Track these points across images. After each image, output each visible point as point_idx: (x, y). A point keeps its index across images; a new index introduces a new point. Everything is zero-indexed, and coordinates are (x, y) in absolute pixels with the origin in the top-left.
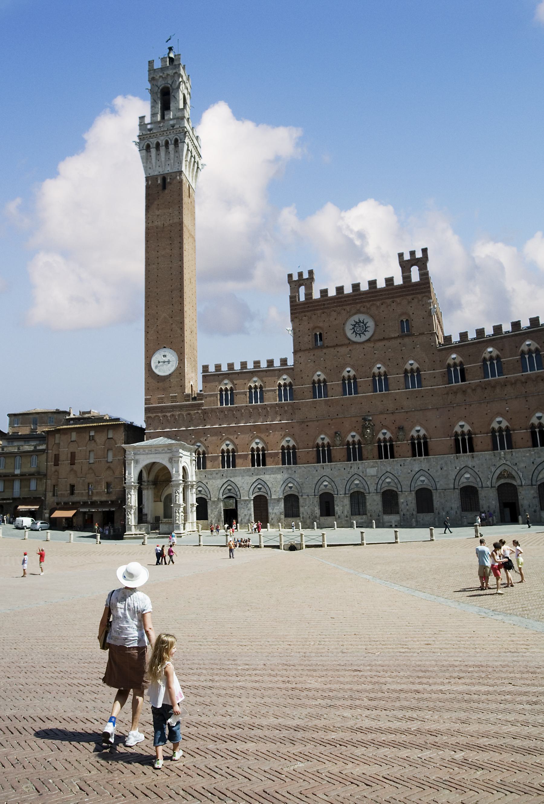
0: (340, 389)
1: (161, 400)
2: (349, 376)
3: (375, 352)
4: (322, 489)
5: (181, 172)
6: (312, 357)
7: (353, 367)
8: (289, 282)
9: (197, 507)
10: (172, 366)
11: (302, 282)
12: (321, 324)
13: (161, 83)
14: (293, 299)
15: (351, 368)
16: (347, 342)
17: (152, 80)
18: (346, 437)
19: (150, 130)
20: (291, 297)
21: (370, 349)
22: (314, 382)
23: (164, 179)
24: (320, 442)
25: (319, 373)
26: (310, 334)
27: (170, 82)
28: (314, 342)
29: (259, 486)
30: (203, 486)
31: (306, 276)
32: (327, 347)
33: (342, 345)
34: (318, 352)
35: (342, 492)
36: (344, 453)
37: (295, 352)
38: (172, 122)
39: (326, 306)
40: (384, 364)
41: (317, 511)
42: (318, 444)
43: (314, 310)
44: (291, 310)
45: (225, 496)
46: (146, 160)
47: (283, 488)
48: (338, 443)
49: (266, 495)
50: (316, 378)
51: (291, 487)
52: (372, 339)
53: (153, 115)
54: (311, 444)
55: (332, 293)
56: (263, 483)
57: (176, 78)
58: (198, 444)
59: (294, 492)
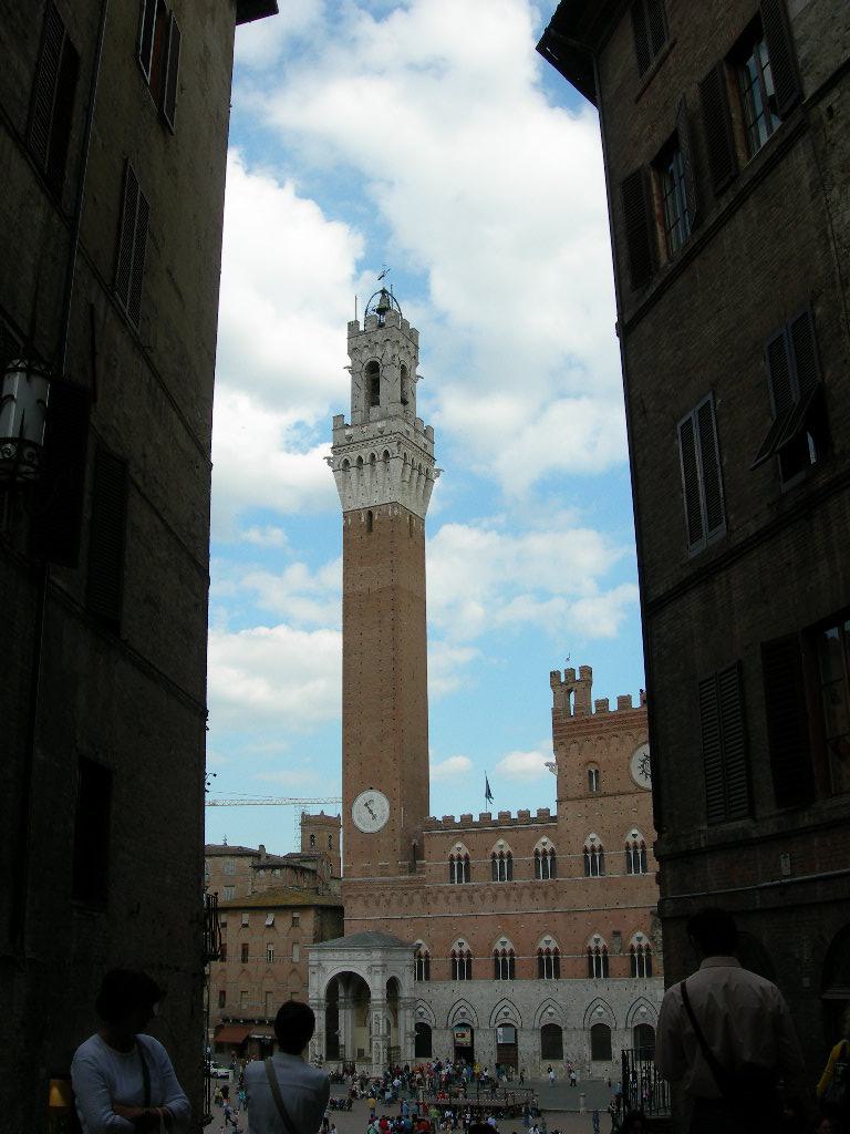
0: (622, 862)
1: (365, 872)
2: (635, 843)
4: (596, 1019)
5: (394, 504)
8: (552, 686)
9: (417, 1038)
10: (382, 818)
13: (367, 357)
16: (632, 788)
17: (353, 351)
18: (629, 938)
19: (349, 438)
20: (555, 712)
22: (586, 851)
23: (370, 514)
24: (592, 945)
25: (593, 836)
27: (379, 354)
28: (588, 785)
29: (505, 1010)
30: (425, 1005)
31: (578, 677)
34: (590, 803)
35: (621, 1025)
36: (626, 964)
38: (379, 425)
39: (604, 728)
41: (587, 1051)
42: (589, 947)
43: (589, 733)
44: (554, 732)
45: (456, 1023)
46: (343, 484)
47: (538, 1017)
48: (617, 948)
49: (514, 1023)
50: (588, 844)
51: (551, 1014)
53: (354, 410)
54: (580, 947)
55: (613, 707)
56: (510, 1005)
57: (388, 347)
58: (419, 941)
59: (556, 1020)
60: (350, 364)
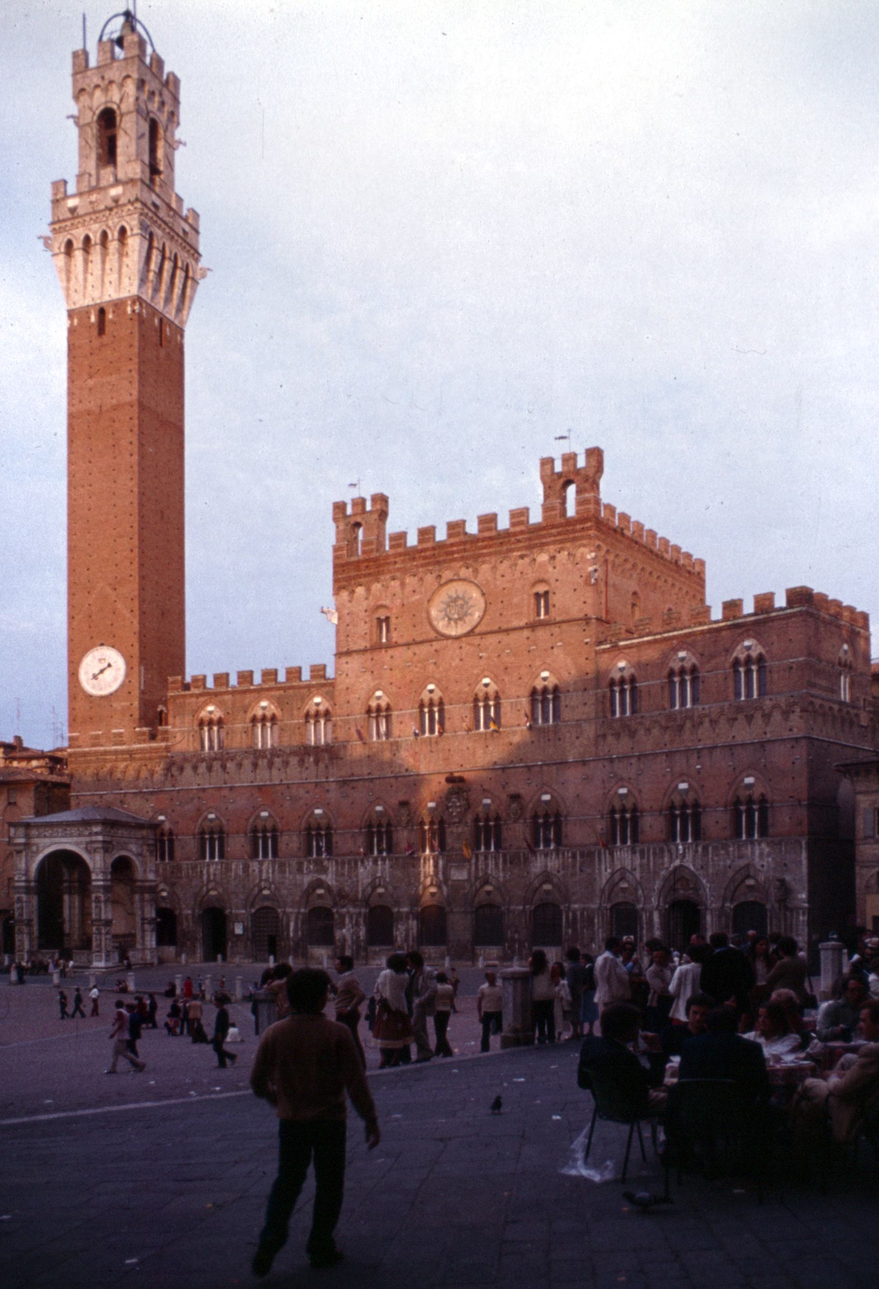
3: (481, 655)
6: (369, 664)
7: (438, 683)
10: (115, 679)
11: (359, 519)
12: (387, 602)
14: (340, 553)
15: (437, 686)
16: (433, 635)
21: (472, 649)
26: (367, 619)
32: (397, 645)
33: (422, 642)
37: (339, 655)
39: (398, 566)
40: (495, 678)
52: (477, 630)
60: (75, 112)
